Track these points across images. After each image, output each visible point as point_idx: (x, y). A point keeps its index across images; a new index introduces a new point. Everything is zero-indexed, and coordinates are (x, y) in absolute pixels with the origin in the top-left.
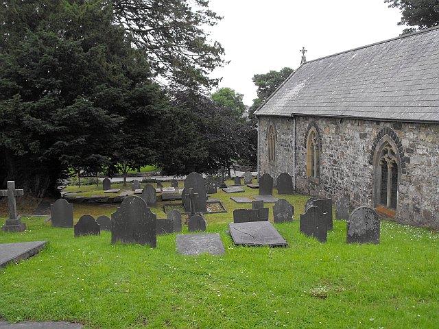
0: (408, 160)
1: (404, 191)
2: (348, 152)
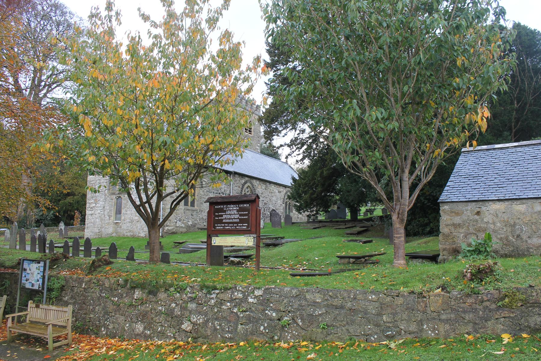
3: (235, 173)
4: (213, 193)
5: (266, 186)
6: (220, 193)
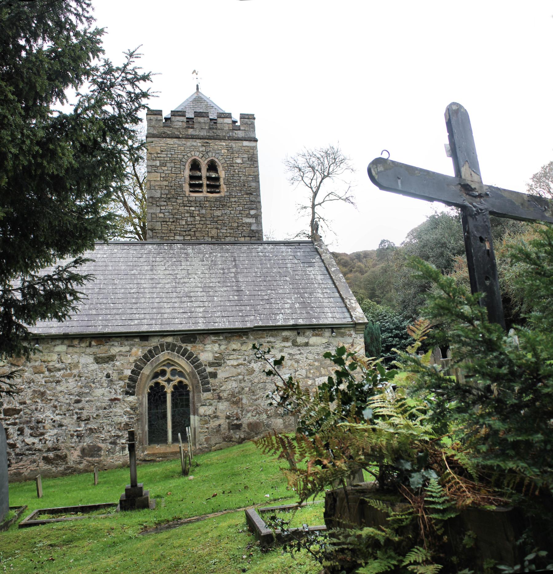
0: (214, 375)
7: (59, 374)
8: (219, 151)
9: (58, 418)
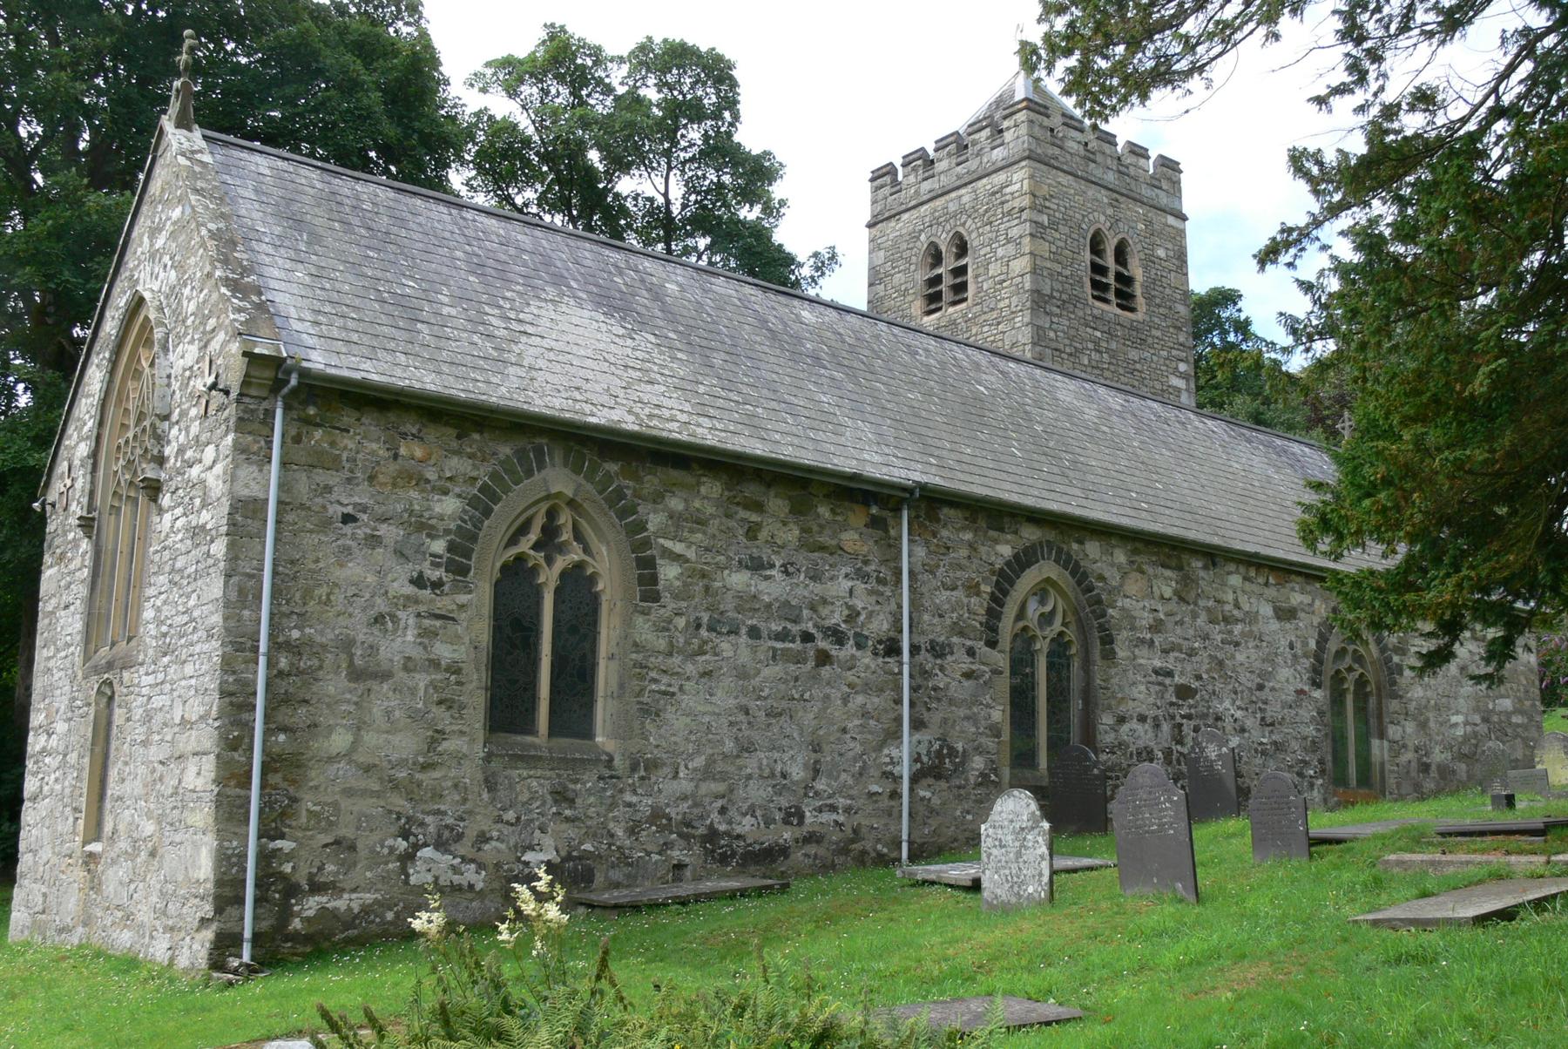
1: (1397, 737)
2: (1240, 657)
3: (930, 503)
4: (754, 633)
5: (1187, 581)
6: (807, 637)
7: (1238, 629)
8: (1133, 223)
9: (1239, 714)
